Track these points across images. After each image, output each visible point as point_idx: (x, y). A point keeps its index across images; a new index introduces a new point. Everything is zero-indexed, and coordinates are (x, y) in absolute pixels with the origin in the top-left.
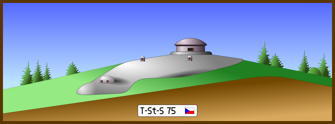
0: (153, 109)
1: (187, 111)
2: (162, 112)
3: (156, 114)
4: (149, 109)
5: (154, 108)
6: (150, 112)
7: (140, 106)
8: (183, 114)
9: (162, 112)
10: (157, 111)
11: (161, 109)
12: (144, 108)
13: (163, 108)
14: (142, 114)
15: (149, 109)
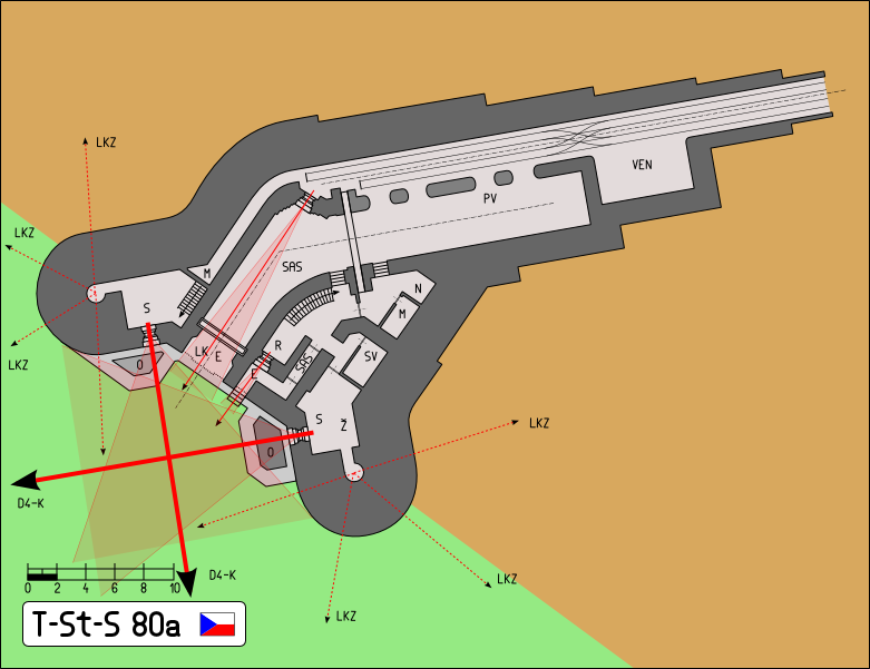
0: (78, 618)
1: (207, 626)
2: (113, 630)
3: (88, 635)
4: (66, 618)
5: (84, 613)
6: (69, 630)
7: (30, 608)
8: (191, 632)
9: (113, 630)
10: (96, 624)
11: (111, 618)
12: (44, 613)
13: (117, 613)
14: (40, 634)
15: (66, 618)
